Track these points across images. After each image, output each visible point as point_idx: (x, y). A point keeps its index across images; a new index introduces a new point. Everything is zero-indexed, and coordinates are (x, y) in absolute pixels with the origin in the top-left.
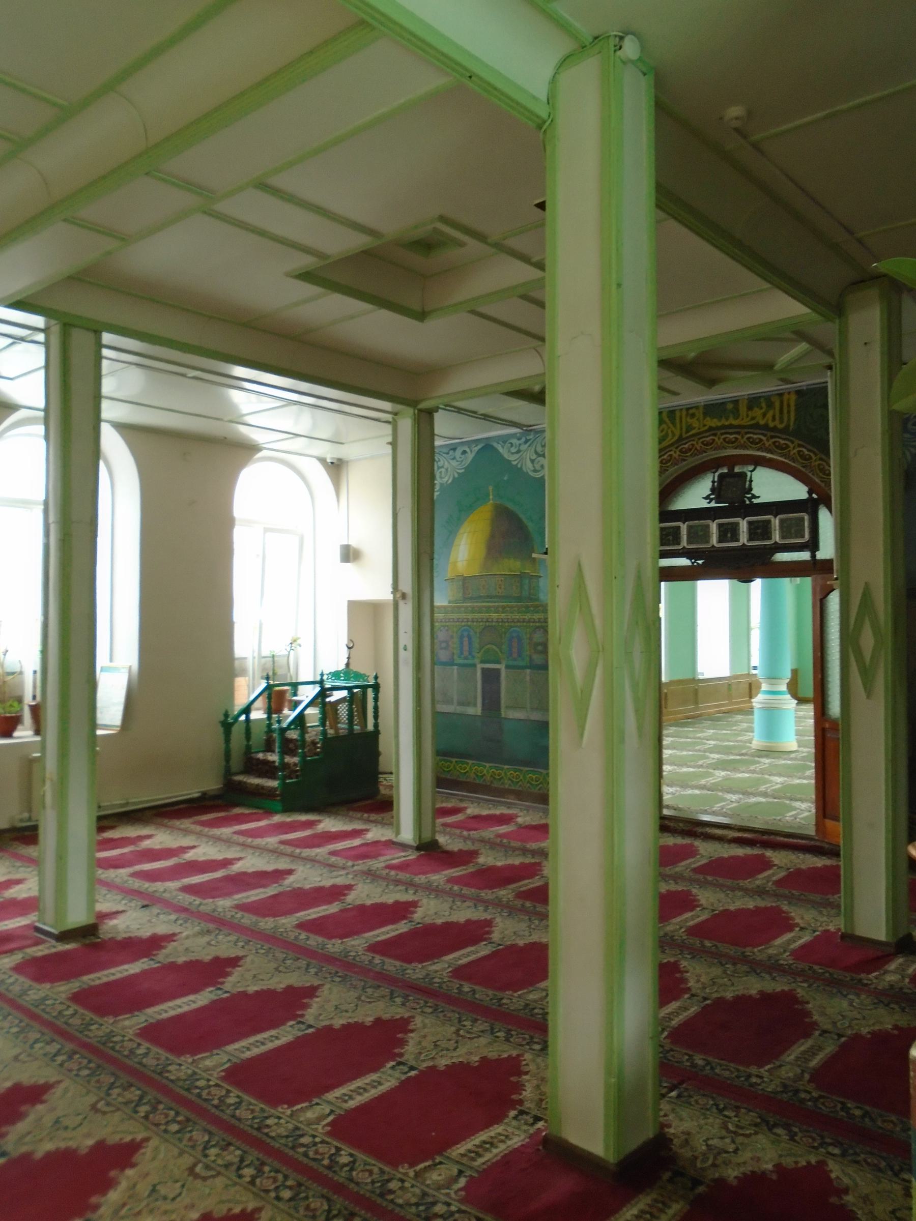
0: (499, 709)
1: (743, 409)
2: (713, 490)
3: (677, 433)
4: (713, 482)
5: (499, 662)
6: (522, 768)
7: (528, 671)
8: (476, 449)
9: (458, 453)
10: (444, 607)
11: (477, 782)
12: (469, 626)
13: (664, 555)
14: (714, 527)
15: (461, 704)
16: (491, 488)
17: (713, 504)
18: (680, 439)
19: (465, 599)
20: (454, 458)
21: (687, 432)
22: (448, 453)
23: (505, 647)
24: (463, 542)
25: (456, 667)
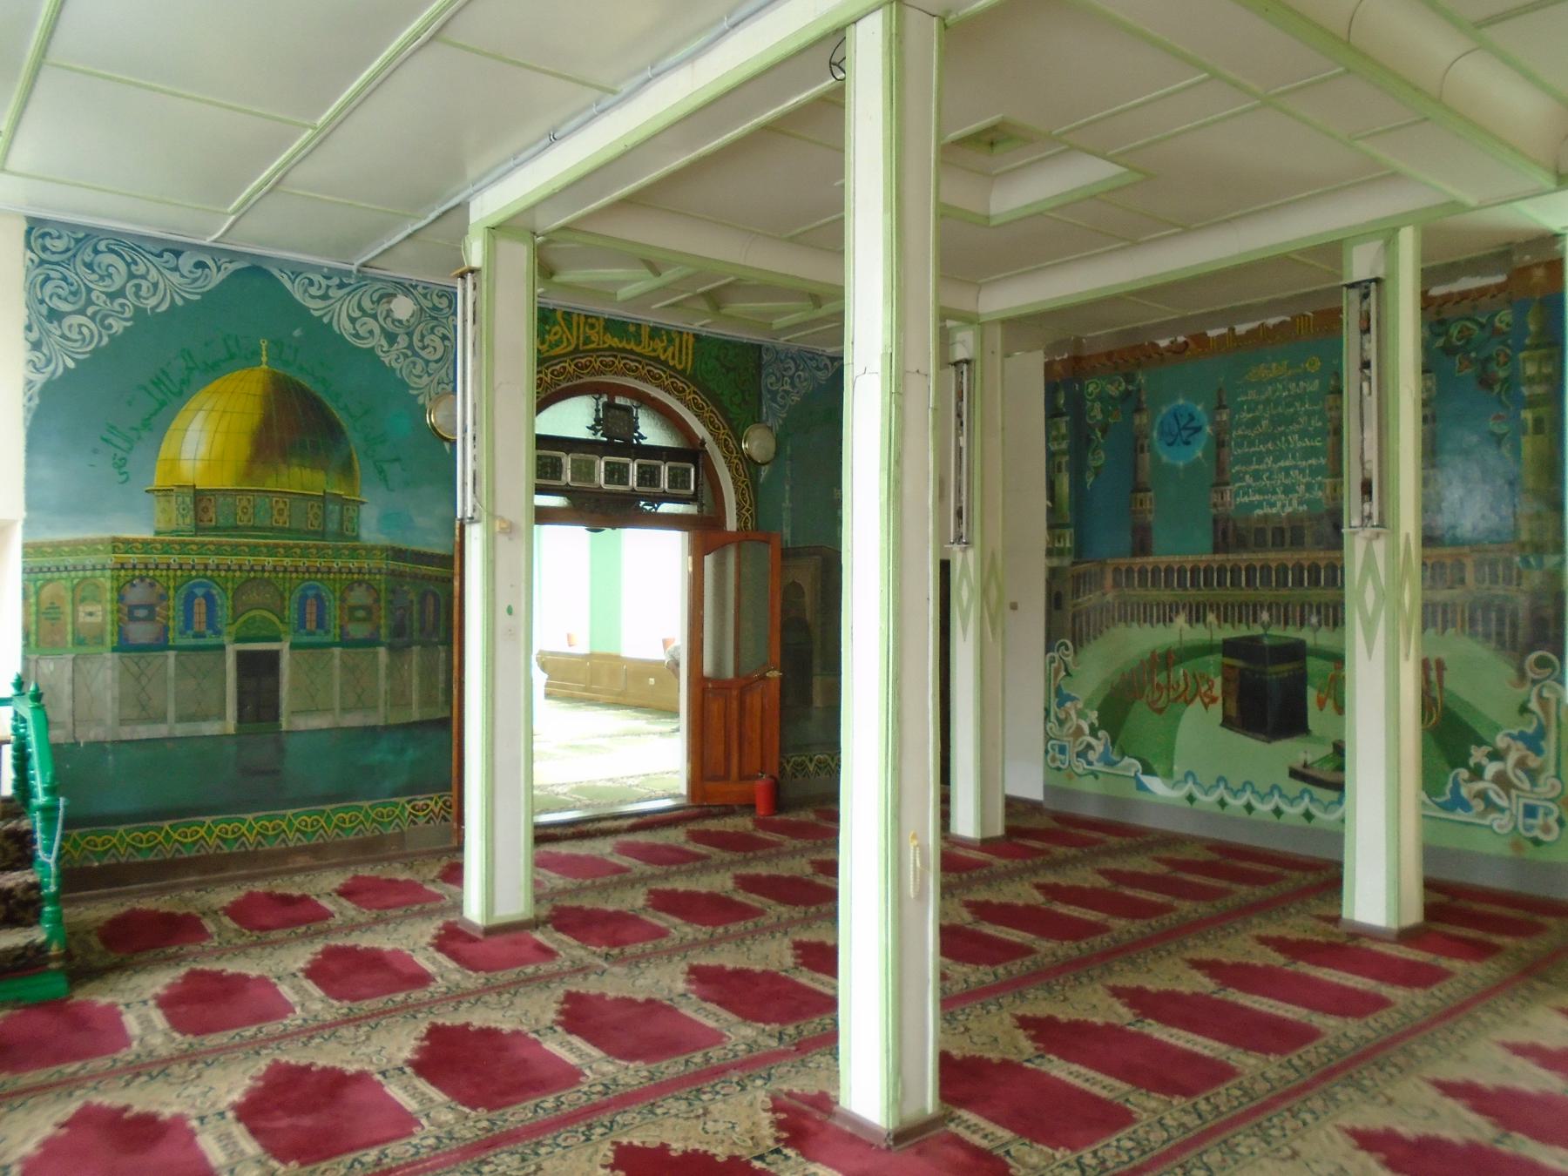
0: (276, 717)
1: (645, 333)
2: (597, 420)
3: (574, 342)
4: (597, 411)
5: (277, 639)
6: (321, 807)
7: (337, 651)
8: (232, 267)
9: (186, 262)
10: (145, 543)
11: (226, 850)
12: (211, 578)
13: (541, 490)
14: (601, 465)
15: (180, 719)
16: (264, 344)
17: (599, 437)
18: (576, 350)
19: (199, 529)
20: (176, 269)
21: (585, 344)
22: (160, 255)
23: (291, 613)
24: (196, 425)
25: (172, 654)
